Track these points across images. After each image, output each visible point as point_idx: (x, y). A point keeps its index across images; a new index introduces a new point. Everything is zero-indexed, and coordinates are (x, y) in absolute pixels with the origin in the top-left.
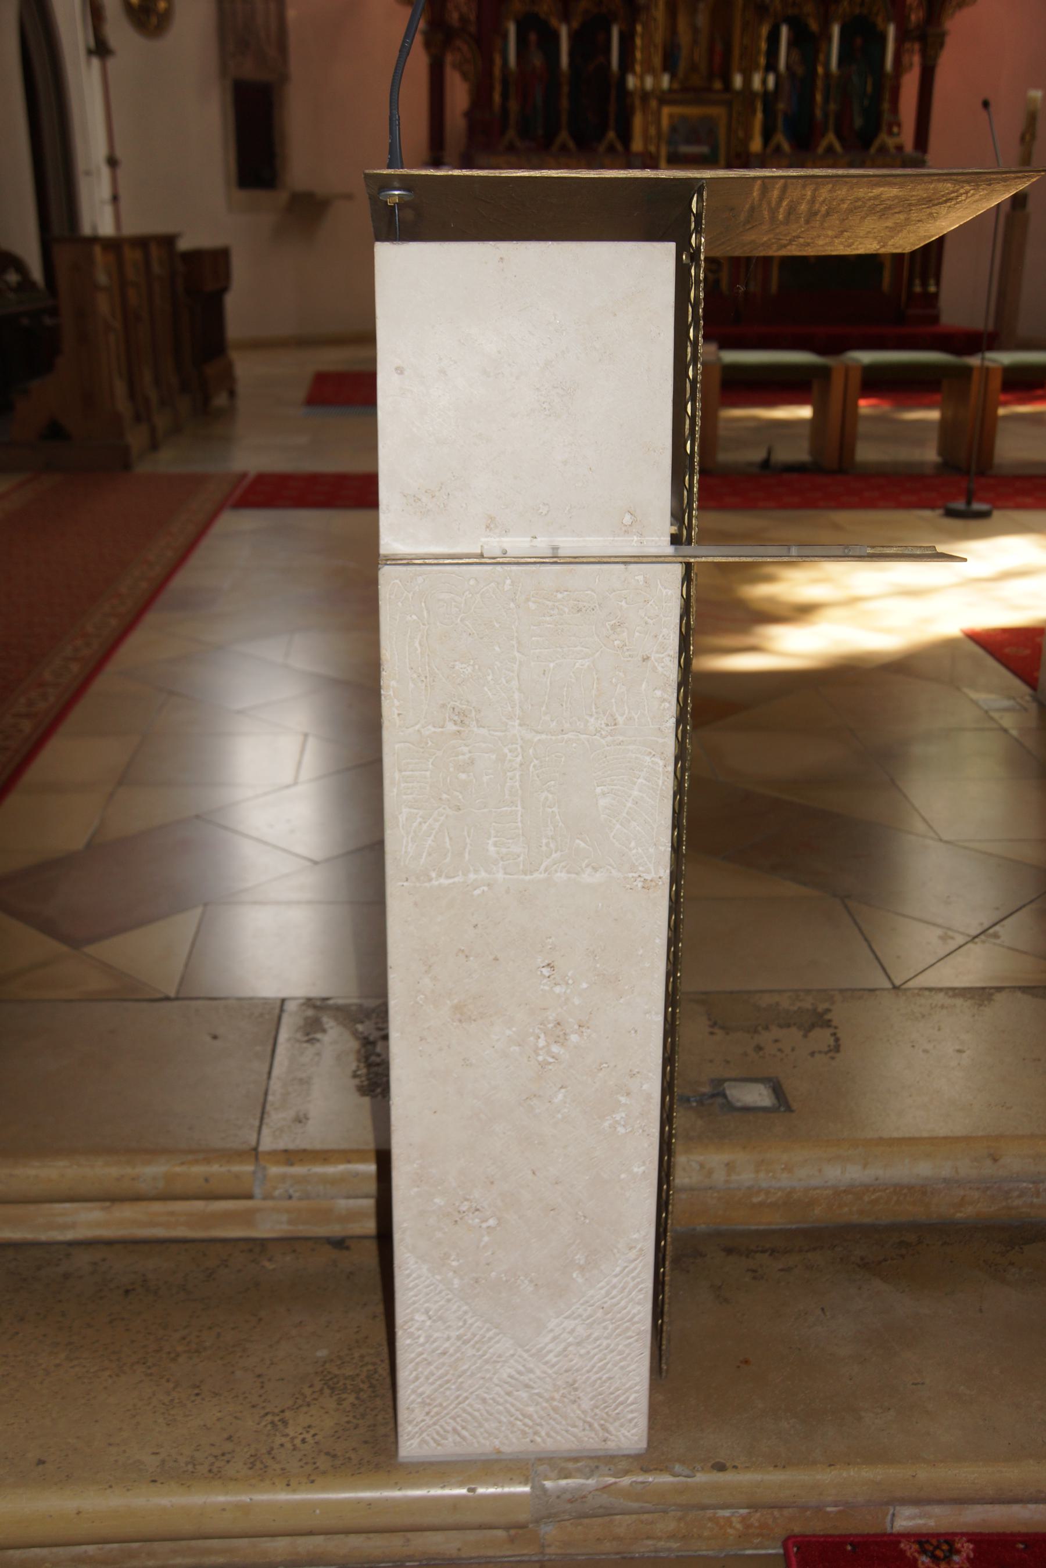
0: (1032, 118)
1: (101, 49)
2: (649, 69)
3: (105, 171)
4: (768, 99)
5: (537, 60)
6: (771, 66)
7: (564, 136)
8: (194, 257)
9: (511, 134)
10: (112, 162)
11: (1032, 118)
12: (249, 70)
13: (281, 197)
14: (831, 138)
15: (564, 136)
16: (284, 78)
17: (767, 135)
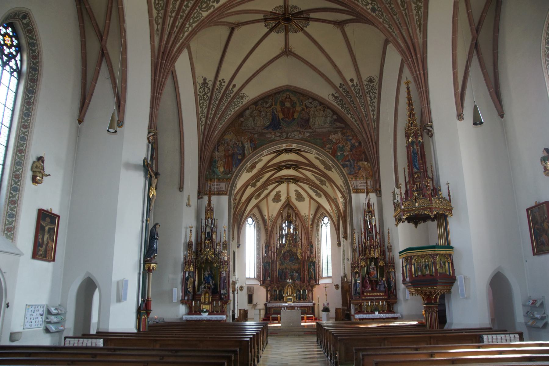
0: (318, 298)
1: (237, 293)
2: (285, 294)
3: (237, 303)
4: (296, 296)
5: (276, 293)
6: (296, 293)
7: (278, 299)
8: (246, 310)
9: (273, 299)
10: (237, 302)
11: (318, 298)
12: (250, 293)
13: (252, 305)
14: (302, 299)
15: (278, 299)
16: (253, 294)
17: (296, 299)
